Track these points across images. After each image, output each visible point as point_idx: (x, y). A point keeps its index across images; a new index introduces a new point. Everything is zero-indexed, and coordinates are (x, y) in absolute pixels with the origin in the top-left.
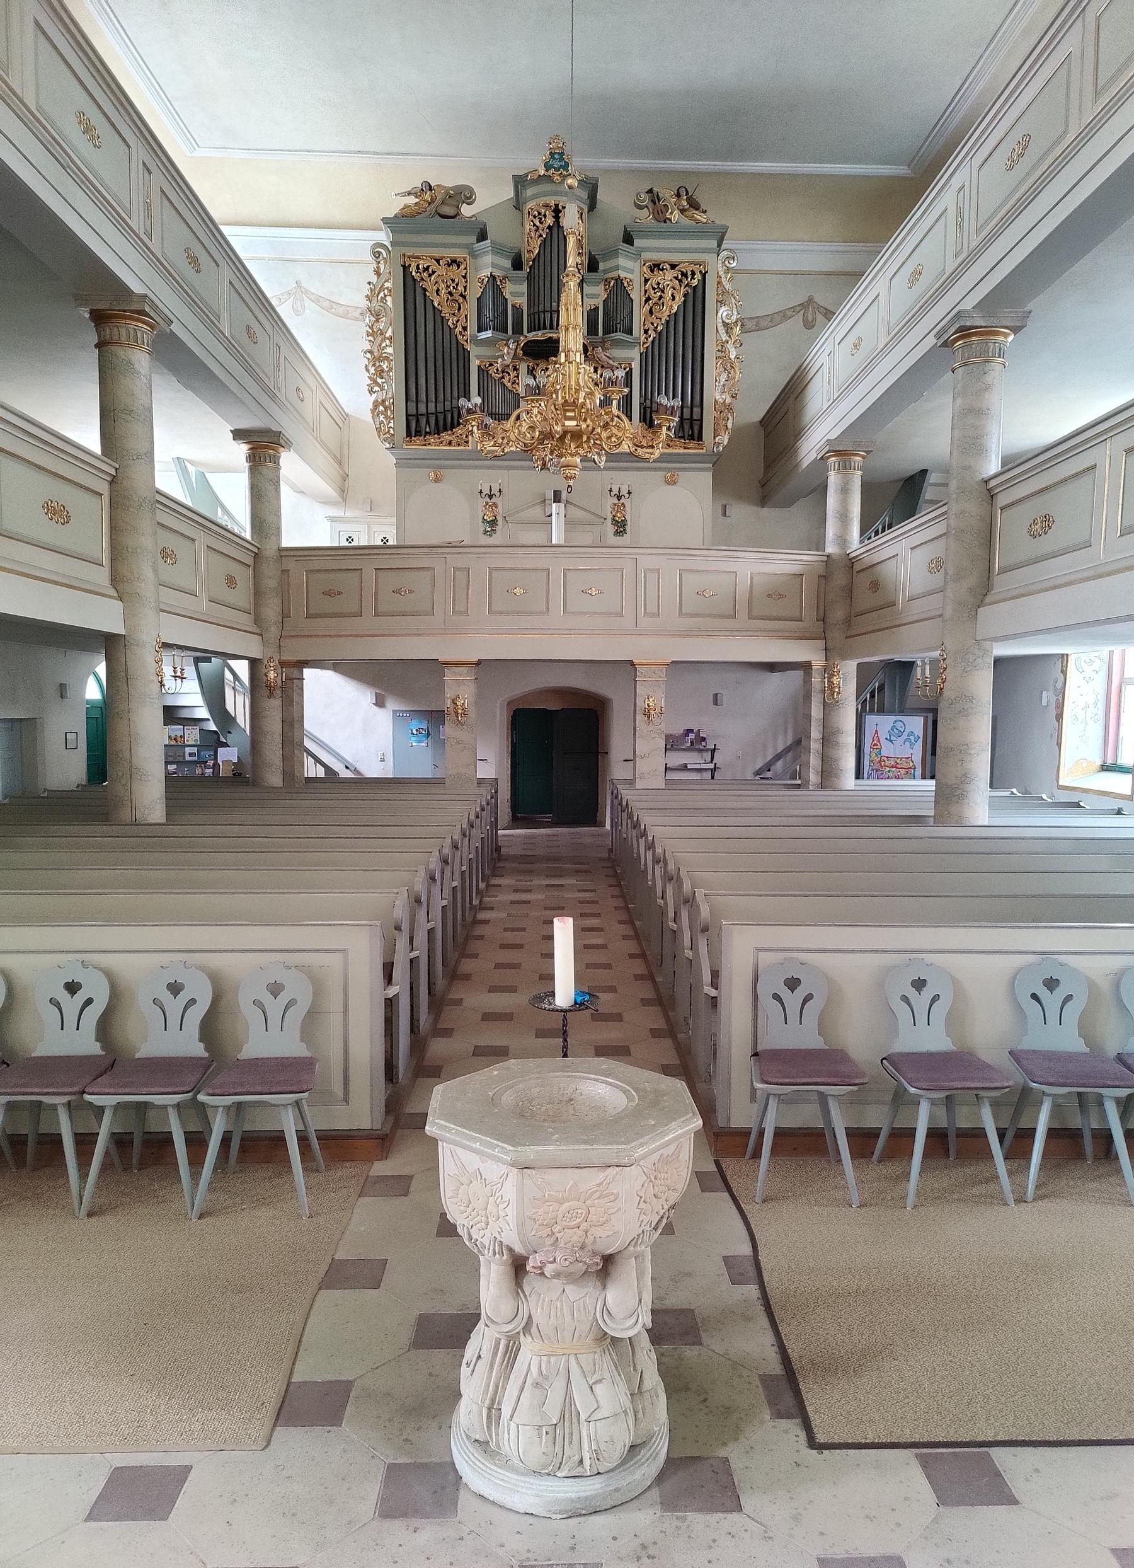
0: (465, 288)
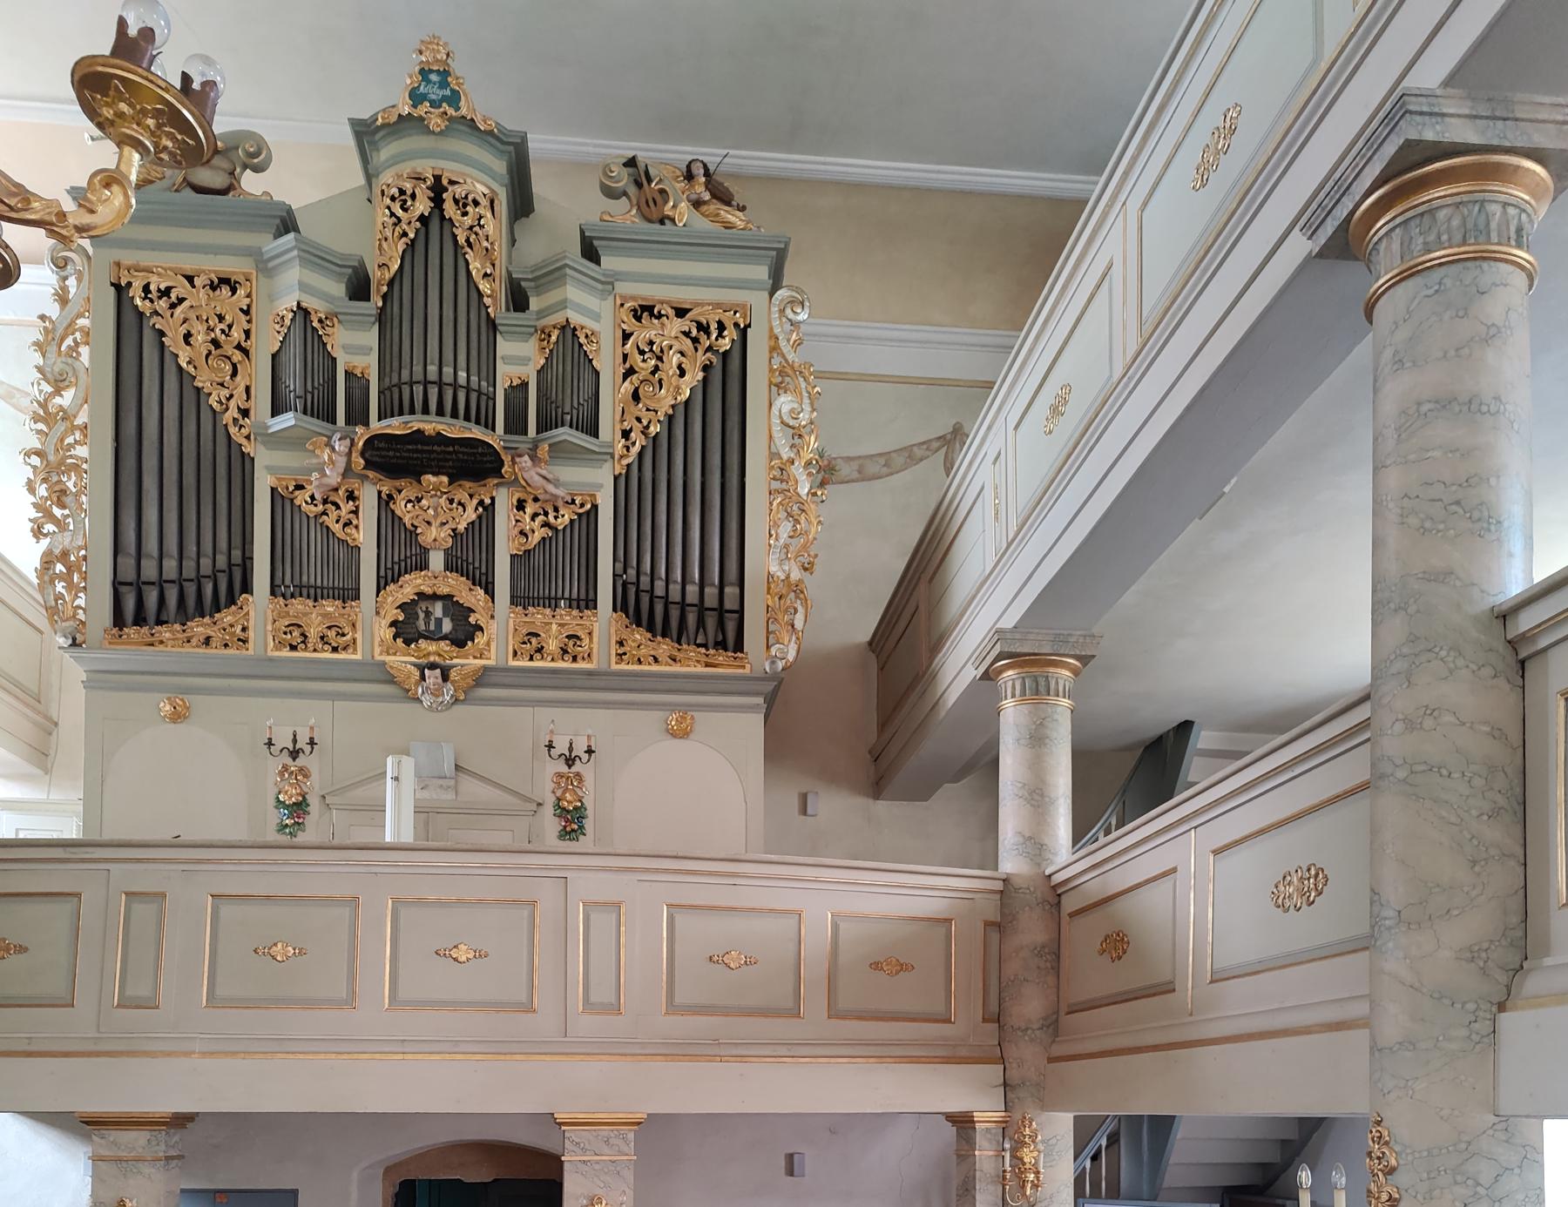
0: (247, 333)
